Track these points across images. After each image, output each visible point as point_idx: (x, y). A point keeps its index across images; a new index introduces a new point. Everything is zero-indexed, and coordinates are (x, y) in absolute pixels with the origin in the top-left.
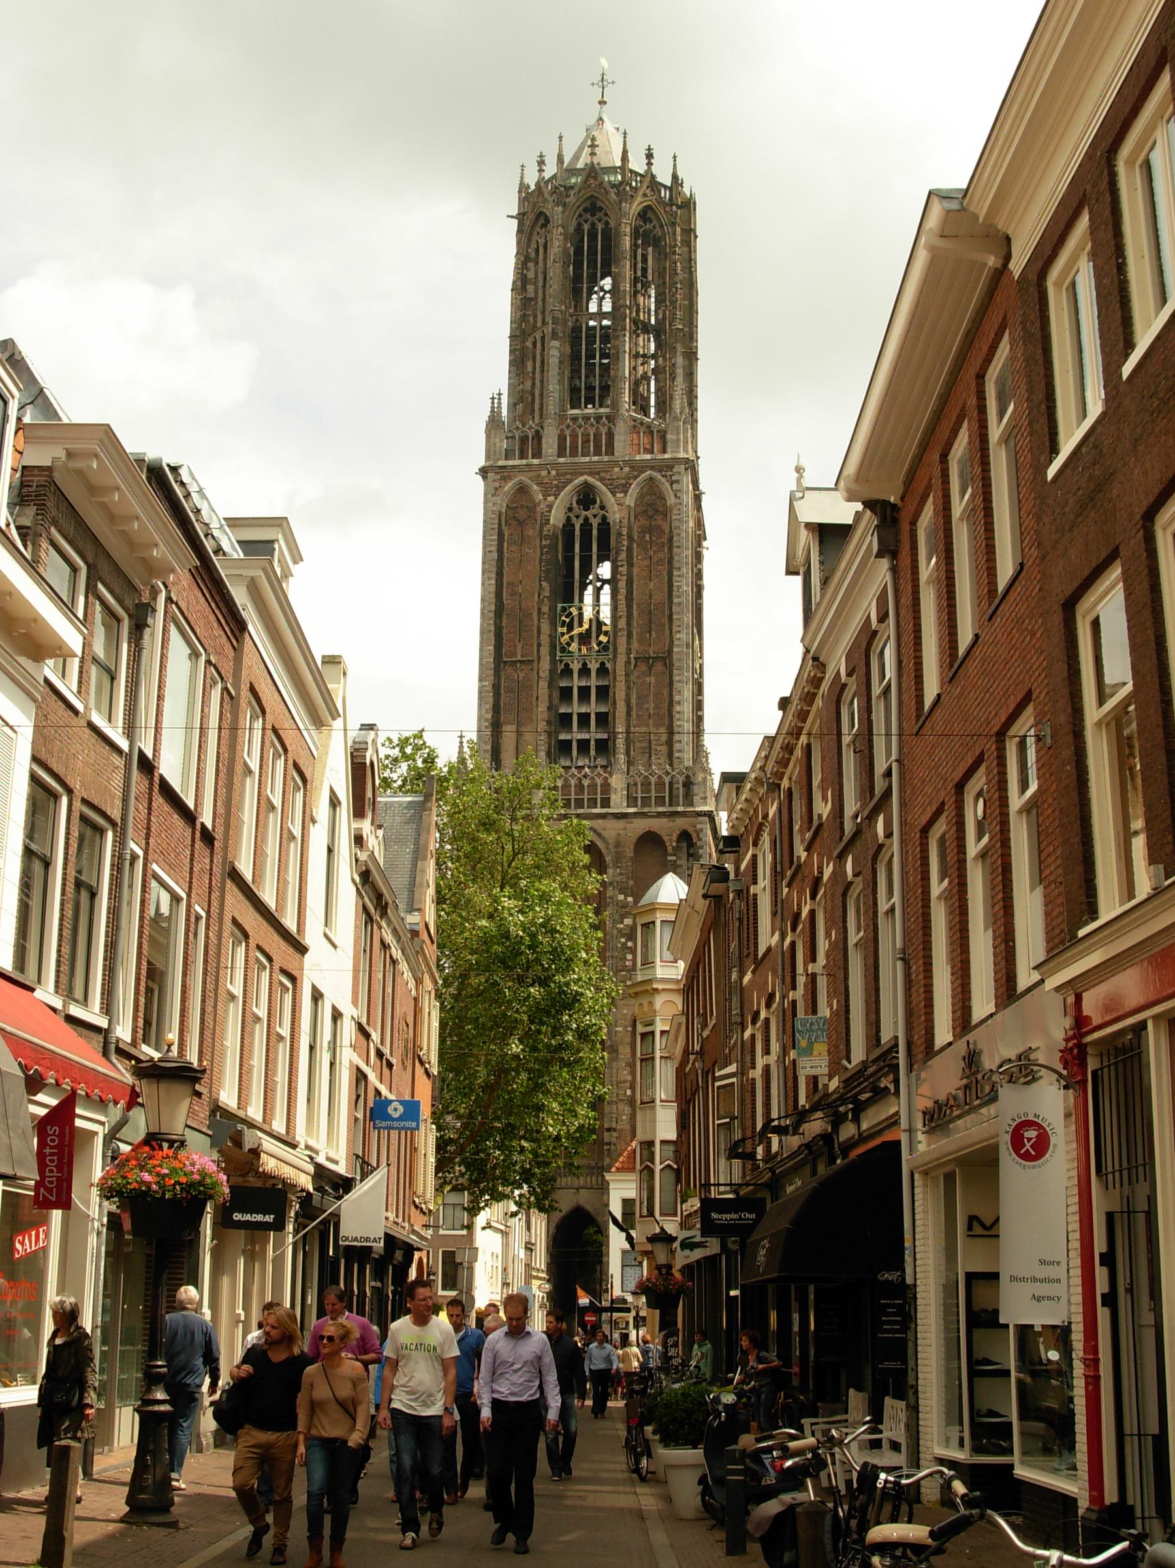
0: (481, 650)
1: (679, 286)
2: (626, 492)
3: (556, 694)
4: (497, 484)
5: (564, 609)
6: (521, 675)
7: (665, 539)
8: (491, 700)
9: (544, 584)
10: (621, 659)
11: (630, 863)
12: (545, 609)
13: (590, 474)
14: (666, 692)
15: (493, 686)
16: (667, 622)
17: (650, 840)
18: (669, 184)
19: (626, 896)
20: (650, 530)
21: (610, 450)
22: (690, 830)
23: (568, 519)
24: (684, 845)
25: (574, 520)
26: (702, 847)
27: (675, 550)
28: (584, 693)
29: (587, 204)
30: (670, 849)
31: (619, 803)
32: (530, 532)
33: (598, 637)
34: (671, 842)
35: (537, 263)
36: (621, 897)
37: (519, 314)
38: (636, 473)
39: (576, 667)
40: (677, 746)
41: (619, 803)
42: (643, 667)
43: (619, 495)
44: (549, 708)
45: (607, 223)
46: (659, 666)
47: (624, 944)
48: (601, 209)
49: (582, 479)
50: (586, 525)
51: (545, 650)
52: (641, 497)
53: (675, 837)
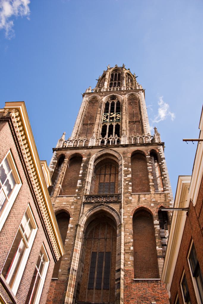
6: (89, 127)
19: (128, 168)
30: (147, 154)
35: (102, 84)
45: (119, 73)
47: (128, 184)
53: (149, 151)
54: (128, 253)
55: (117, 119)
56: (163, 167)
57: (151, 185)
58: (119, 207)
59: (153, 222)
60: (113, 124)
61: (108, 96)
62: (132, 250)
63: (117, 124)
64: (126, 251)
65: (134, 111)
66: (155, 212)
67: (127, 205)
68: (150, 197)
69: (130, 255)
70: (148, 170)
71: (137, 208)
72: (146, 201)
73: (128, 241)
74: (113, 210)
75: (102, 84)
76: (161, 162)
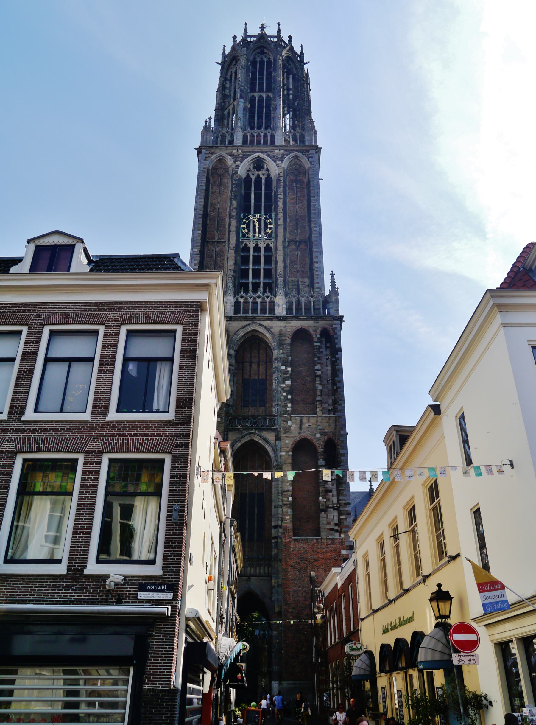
0: (193, 234)
1: (306, 93)
2: (282, 161)
3: (239, 258)
4: (207, 155)
5: (245, 216)
7: (305, 186)
8: (198, 259)
9: (234, 202)
10: (280, 240)
11: (289, 347)
12: (234, 214)
13: (261, 152)
14: (307, 259)
15: (200, 251)
16: (306, 224)
18: (299, 53)
19: (287, 367)
20: (296, 181)
22: (328, 328)
23: (248, 175)
24: (324, 340)
25: (251, 176)
26: (337, 338)
27: (312, 188)
29: (259, 50)
30: (315, 339)
31: (281, 311)
32: (226, 181)
33: (265, 230)
34: (316, 335)
35: (230, 82)
36: (283, 367)
37: (220, 102)
38: (287, 153)
39: (251, 245)
41: (281, 311)
42: (293, 247)
43: (278, 162)
44: (235, 264)
45: (269, 59)
46: (302, 246)
47: (286, 398)
48: (266, 53)
49: (255, 155)
50: (258, 179)
51: (233, 234)
52: (290, 165)
53: (318, 332)
54: (286, 505)
55: (267, 233)
56: (337, 367)
57: (318, 401)
58: (274, 438)
59: (317, 463)
60: (260, 245)
61: (249, 158)
62: (290, 501)
63: (268, 245)
64: (284, 503)
65: (299, 210)
66: (320, 446)
67: (285, 435)
68: (315, 422)
69: (289, 507)
70: (316, 372)
71: (298, 439)
72: (310, 429)
73: (286, 489)
74: (267, 442)
75: (230, 82)
76: (335, 357)
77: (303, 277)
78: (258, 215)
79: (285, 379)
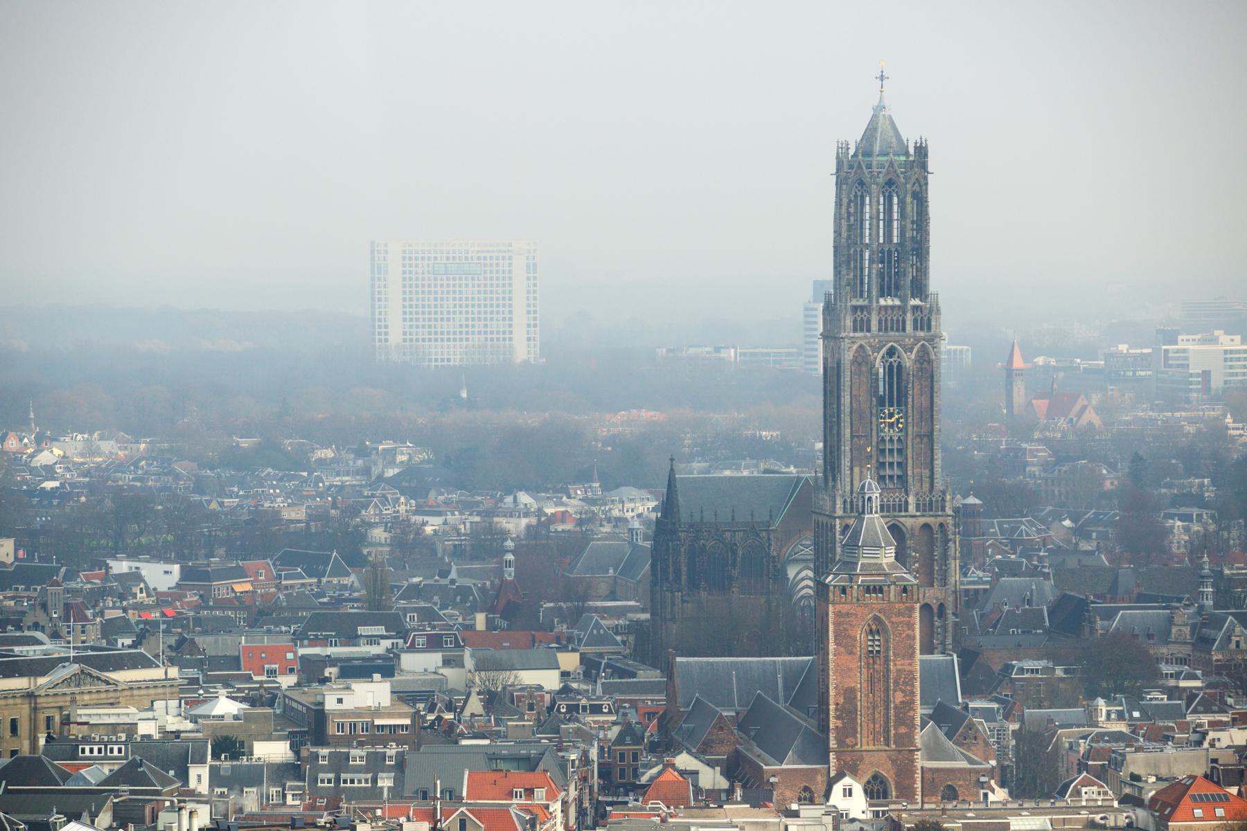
2: (911, 352)
9: (874, 399)
10: (910, 438)
13: (894, 342)
14: (929, 452)
17: (926, 526)
21: (904, 330)
28: (891, 451)
34: (936, 528)
36: (914, 554)
39: (888, 438)
40: (936, 481)
42: (918, 439)
43: (909, 354)
51: (874, 433)
52: (917, 355)
66: (935, 608)
77: (925, 469)
78: (891, 409)
79: (915, 563)
